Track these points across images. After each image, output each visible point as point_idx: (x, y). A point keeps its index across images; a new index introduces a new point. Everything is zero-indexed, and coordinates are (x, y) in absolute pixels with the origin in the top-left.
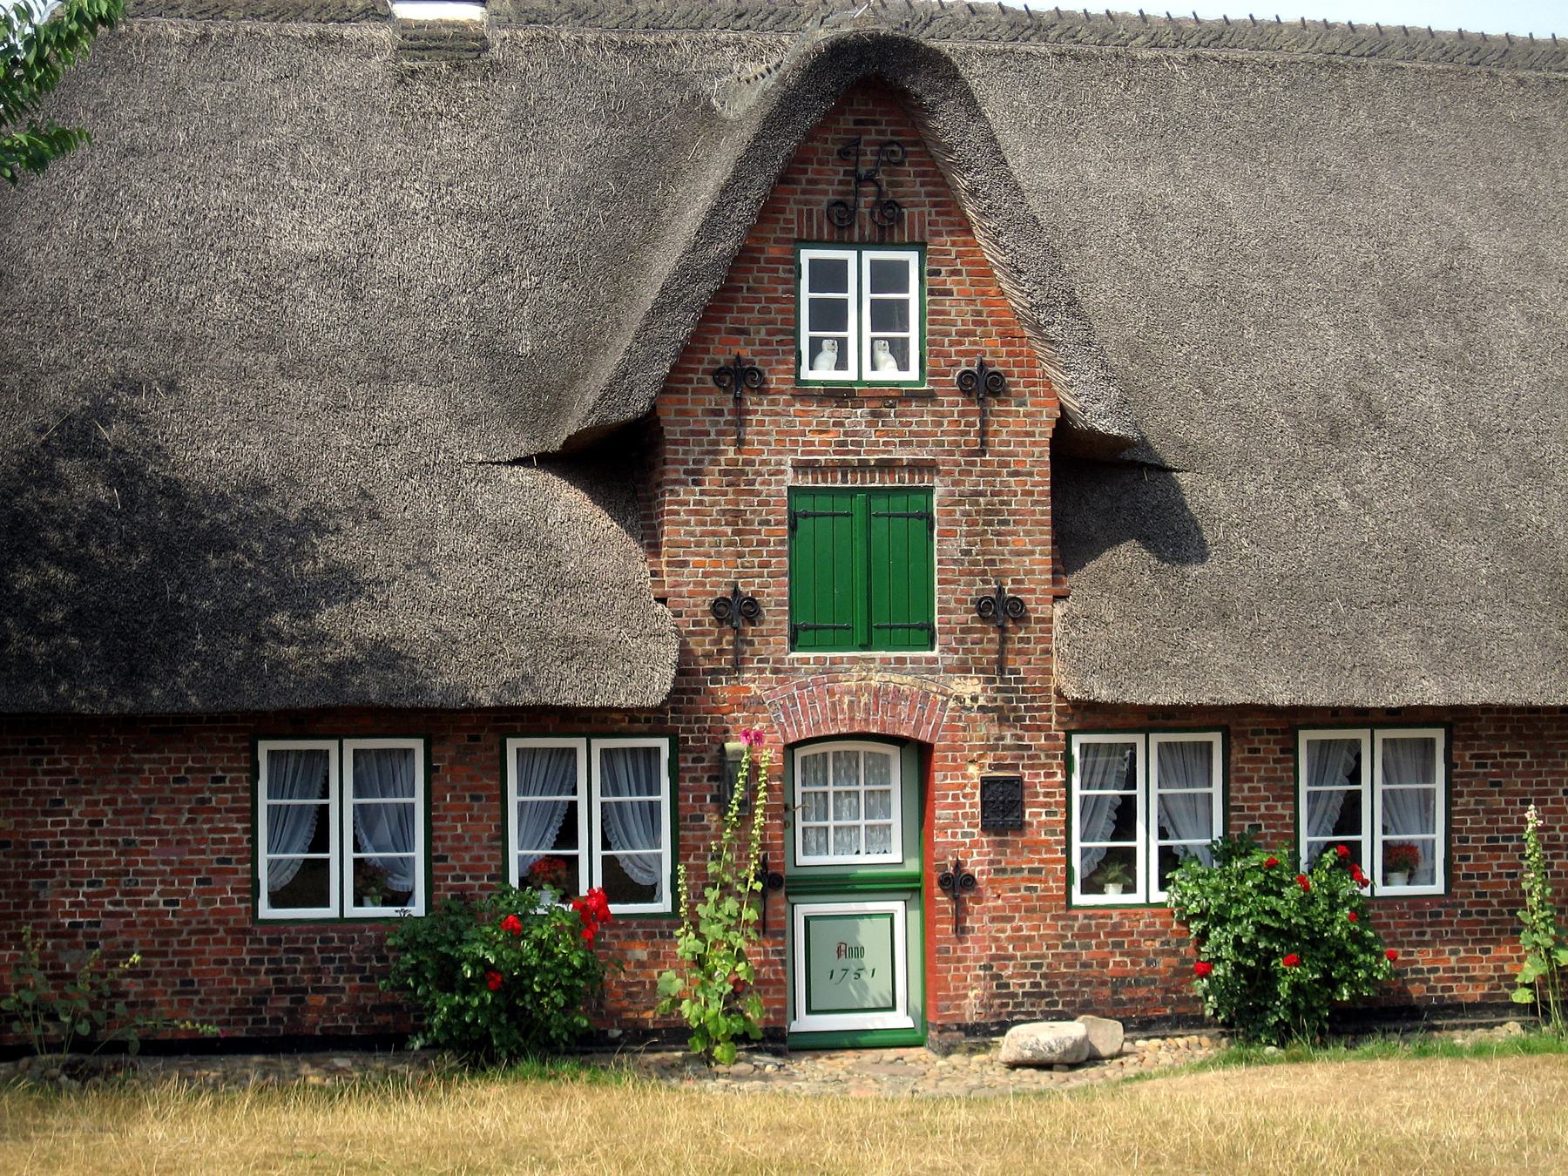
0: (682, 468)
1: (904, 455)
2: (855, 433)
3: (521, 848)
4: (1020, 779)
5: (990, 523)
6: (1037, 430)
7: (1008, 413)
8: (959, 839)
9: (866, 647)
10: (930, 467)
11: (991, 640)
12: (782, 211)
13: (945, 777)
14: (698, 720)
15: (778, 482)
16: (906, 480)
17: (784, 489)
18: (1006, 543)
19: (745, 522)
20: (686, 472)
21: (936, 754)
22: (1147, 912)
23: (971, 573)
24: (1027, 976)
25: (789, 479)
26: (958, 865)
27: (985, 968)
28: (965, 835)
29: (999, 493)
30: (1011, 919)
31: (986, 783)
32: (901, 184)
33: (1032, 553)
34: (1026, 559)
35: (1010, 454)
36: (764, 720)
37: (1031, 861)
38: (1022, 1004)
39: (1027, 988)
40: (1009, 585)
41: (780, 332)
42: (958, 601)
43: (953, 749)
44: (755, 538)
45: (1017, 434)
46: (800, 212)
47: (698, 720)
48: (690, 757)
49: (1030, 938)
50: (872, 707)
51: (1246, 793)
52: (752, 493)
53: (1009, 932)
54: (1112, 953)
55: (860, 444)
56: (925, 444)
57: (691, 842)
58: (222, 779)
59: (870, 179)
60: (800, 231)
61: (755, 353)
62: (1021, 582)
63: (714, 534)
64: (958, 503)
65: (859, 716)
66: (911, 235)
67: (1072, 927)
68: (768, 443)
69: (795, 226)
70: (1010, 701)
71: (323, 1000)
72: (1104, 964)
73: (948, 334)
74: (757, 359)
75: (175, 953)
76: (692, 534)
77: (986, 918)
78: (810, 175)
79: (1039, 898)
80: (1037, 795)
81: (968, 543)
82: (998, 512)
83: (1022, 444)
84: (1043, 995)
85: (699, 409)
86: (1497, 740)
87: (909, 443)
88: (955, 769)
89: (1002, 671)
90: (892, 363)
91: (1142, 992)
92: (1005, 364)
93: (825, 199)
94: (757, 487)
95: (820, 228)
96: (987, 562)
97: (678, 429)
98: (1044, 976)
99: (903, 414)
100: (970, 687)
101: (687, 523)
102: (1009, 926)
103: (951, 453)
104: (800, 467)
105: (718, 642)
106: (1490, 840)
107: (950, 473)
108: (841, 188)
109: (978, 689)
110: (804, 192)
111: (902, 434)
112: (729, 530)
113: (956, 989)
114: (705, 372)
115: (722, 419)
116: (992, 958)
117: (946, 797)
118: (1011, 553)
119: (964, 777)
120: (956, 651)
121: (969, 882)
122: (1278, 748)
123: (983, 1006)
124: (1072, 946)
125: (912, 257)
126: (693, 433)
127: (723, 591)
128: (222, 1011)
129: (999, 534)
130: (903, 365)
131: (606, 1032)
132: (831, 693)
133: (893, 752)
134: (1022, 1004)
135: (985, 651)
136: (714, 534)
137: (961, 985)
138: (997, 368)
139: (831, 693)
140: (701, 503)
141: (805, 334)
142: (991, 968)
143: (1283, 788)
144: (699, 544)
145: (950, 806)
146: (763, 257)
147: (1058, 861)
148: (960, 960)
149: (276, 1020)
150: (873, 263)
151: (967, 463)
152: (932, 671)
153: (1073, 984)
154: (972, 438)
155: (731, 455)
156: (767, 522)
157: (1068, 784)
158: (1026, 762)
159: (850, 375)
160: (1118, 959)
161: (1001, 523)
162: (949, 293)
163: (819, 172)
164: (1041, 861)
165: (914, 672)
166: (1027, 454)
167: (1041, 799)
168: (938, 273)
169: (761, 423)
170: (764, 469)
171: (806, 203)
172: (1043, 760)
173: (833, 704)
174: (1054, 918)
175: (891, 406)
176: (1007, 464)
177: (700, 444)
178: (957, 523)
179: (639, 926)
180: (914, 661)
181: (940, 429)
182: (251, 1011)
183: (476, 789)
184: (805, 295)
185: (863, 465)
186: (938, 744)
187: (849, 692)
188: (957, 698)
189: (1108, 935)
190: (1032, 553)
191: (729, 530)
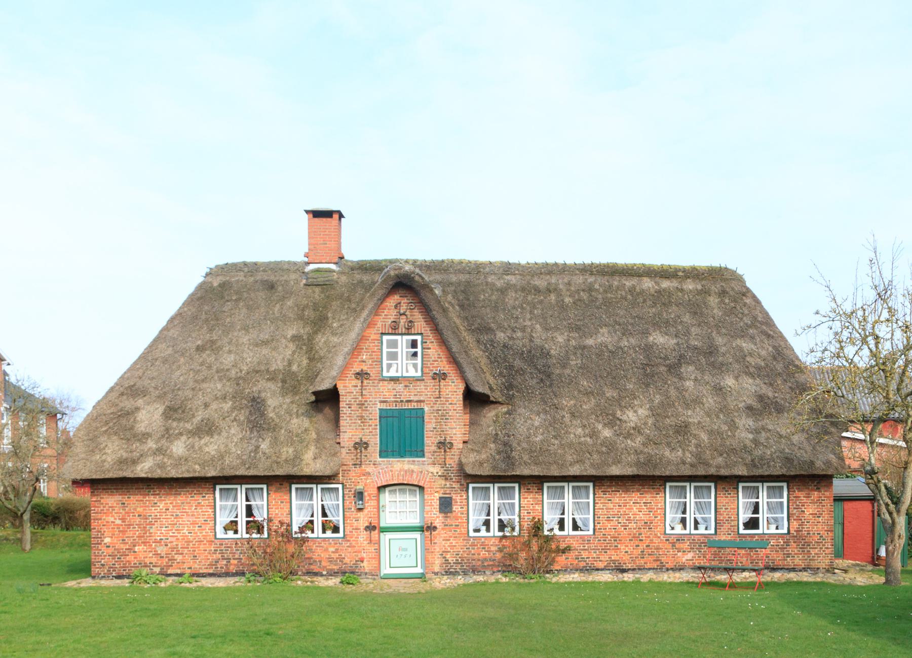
1: (416, 399)
4: (451, 498)
9: (402, 457)
10: (423, 401)
16: (414, 405)
25: (379, 406)
31: (440, 498)
59: (404, 314)
71: (236, 562)
90: (413, 370)
91: (491, 563)
104: (381, 402)
121: (435, 528)
125: (419, 338)
127: (358, 440)
130: (416, 371)
133: (417, 489)
141: (385, 362)
157: (468, 499)
159: (399, 374)
181: (426, 391)
184: (385, 350)
185: (402, 401)
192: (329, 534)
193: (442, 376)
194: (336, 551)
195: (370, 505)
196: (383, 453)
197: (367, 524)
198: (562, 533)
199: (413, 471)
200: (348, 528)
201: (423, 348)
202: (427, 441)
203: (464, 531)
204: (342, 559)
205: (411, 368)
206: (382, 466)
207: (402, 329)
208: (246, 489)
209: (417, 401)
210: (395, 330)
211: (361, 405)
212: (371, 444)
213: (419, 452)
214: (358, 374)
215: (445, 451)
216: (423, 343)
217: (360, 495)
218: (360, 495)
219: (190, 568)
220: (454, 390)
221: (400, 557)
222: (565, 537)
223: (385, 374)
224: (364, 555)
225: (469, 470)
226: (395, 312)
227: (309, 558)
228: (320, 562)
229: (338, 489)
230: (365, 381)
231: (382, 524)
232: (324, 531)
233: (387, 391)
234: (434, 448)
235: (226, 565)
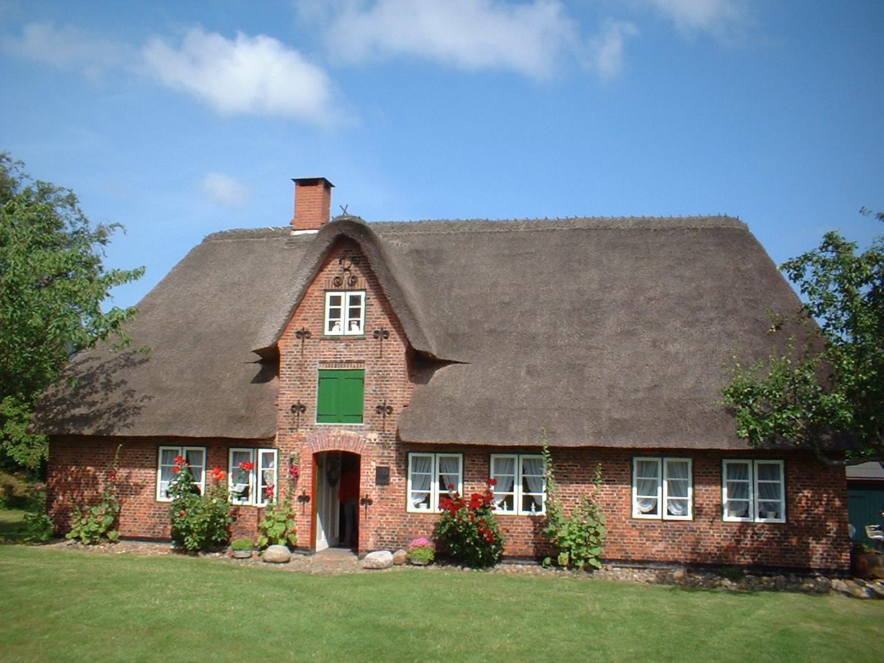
1: (355, 359)
5: (382, 381)
8: (369, 487)
10: (363, 362)
11: (381, 420)
15: (315, 368)
17: (316, 370)
19: (304, 381)
20: (287, 365)
21: (362, 458)
22: (433, 516)
26: (367, 496)
27: (376, 531)
28: (370, 486)
29: (386, 371)
31: (378, 468)
35: (391, 358)
39: (390, 539)
40: (388, 402)
41: (318, 319)
42: (371, 407)
43: (367, 456)
44: (306, 385)
45: (393, 351)
47: (286, 444)
49: (391, 522)
51: (470, 476)
53: (384, 520)
57: (283, 484)
58: (147, 458)
61: (310, 326)
62: (392, 401)
65: (337, 444)
66: (361, 286)
70: (386, 441)
73: (371, 318)
75: (133, 510)
76: (286, 384)
77: (377, 514)
79: (395, 508)
82: (386, 377)
83: (395, 354)
86: (566, 460)
89: (384, 431)
93: (334, 277)
94: (308, 369)
98: (396, 535)
100: (374, 436)
101: (285, 381)
102: (384, 517)
104: (321, 362)
106: (563, 497)
109: (376, 437)
111: (355, 352)
114: (294, 333)
116: (378, 528)
117: (364, 472)
118: (390, 391)
119: (371, 466)
120: (369, 424)
122: (482, 460)
123: (374, 544)
124: (406, 526)
125: (363, 294)
126: (289, 352)
128: (143, 529)
132: (328, 437)
135: (379, 424)
136: (294, 384)
139: (328, 437)
141: (327, 320)
143: (484, 475)
144: (289, 387)
146: (313, 296)
147: (402, 496)
149: (159, 532)
152: (361, 430)
153: (405, 539)
154: (378, 352)
155: (300, 359)
156: (310, 381)
159: (341, 333)
160: (422, 531)
162: (372, 305)
164: (396, 496)
165: (354, 431)
168: (369, 298)
171: (328, 278)
176: (389, 361)
177: (291, 356)
180: (356, 427)
182: (152, 529)
185: (342, 362)
186: (362, 454)
187: (334, 436)
188: (369, 440)
189: (419, 523)
191: (298, 383)
193: (386, 334)
196: (320, 417)
198: (510, 513)
201: (366, 305)
202: (367, 405)
203: (401, 505)
207: (345, 285)
208: (187, 451)
209: (357, 362)
210: (338, 284)
213: (359, 417)
214: (298, 333)
215: (384, 416)
216: (366, 299)
219: (129, 531)
220: (396, 351)
222: (512, 518)
223: (327, 332)
224: (297, 527)
225: (404, 438)
227: (241, 528)
233: (328, 352)
234: (373, 412)
235: (163, 530)
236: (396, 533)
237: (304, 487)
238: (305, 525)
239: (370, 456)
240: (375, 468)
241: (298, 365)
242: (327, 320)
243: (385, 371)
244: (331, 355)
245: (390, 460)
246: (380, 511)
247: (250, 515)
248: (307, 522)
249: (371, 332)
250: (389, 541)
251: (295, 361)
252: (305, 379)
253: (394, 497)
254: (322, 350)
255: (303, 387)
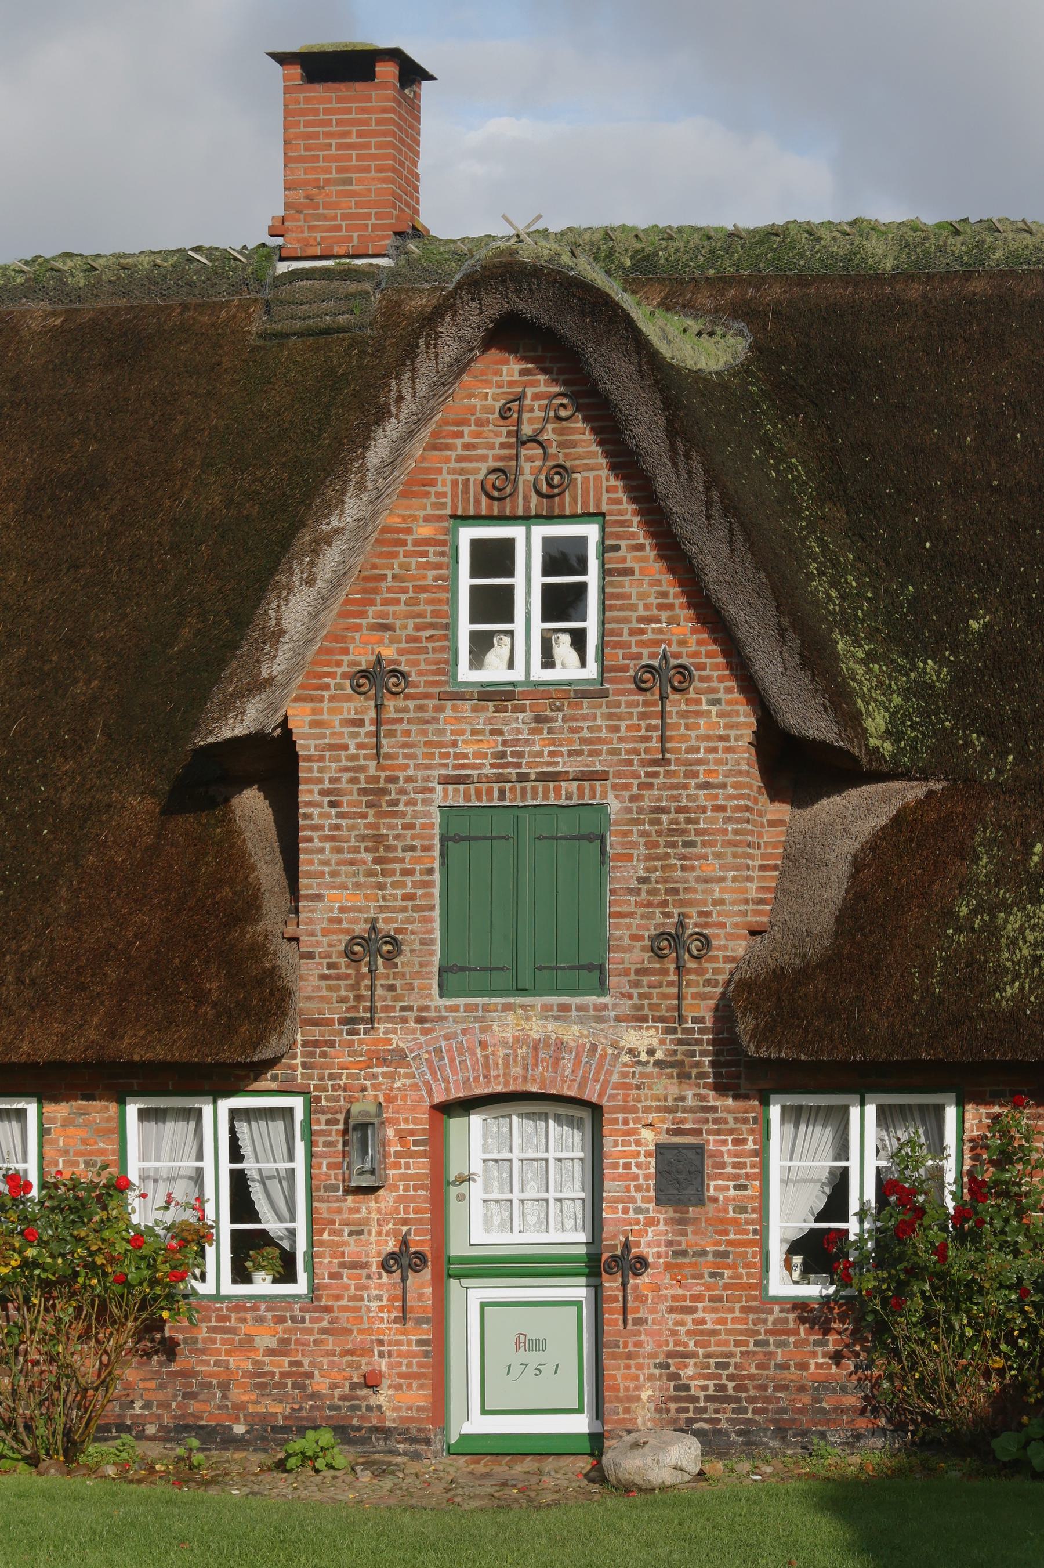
0: (316, 788)
1: (573, 766)
2: (516, 742)
3: (233, 1221)
5: (673, 845)
6: (732, 733)
7: (698, 714)
10: (603, 776)
11: (670, 984)
12: (433, 483)
13: (616, 1145)
14: (331, 1077)
18: (693, 868)
19: (388, 848)
20: (322, 793)
23: (649, 904)
24: (709, 1377)
25: (439, 796)
26: (627, 1245)
28: (638, 1210)
30: (692, 1310)
32: (574, 444)
33: (723, 879)
34: (716, 887)
35: (700, 762)
36: (407, 1076)
37: (719, 1243)
38: (704, 1410)
39: (711, 1392)
42: (635, 938)
43: (625, 1109)
45: (708, 738)
46: (455, 483)
47: (331, 1077)
48: (323, 1118)
49: (714, 1333)
50: (530, 1061)
52: (395, 814)
53: (690, 1326)
54: (814, 1354)
55: (520, 755)
56: (598, 753)
57: (325, 1215)
60: (454, 506)
61: (401, 652)
62: (707, 914)
63: (352, 863)
64: (638, 822)
66: (586, 503)
67: (765, 1322)
68: (412, 756)
69: (448, 500)
70: (692, 1054)
72: (803, 1366)
74: (403, 659)
76: (326, 863)
78: (467, 439)
79: (726, 1287)
80: (723, 1165)
81: (647, 869)
82: (684, 832)
83: (715, 750)
84: (727, 1400)
85: (337, 719)
87: (579, 753)
88: (629, 1133)
90: (573, 656)
92: (696, 654)
94: (401, 807)
95: (478, 502)
96: (668, 891)
97: (312, 743)
98: (731, 1378)
99: (574, 719)
100: (644, 1039)
101: (322, 851)
102: (689, 1318)
103: (630, 763)
104: (446, 780)
105: (355, 987)
107: (627, 787)
108: (503, 452)
109: (655, 1042)
110: (460, 459)
112: (369, 857)
113: (627, 1389)
114: (344, 675)
115: (362, 731)
116: (670, 1355)
117: (615, 1166)
118: (698, 880)
119: (638, 1143)
120: (630, 997)
121: (642, 1262)
125: (591, 531)
129: (684, 857)
130: (583, 664)
131: (230, 1428)
133: (586, 1115)
134: (704, 1410)
135: (665, 996)
136: (352, 863)
137: (632, 1384)
138: (685, 661)
139: (483, 1045)
140: (337, 827)
141: (465, 627)
142: (668, 1366)
144: (334, 874)
145: (621, 1177)
146: (410, 538)
147: (751, 1243)
148: (629, 1356)
150: (547, 541)
151: (648, 775)
152: (600, 1020)
155: (372, 771)
156: (413, 848)
157: (762, 1153)
158: (711, 1126)
159: (517, 675)
161: (687, 844)
163: (478, 435)
164: (729, 1243)
165: (581, 1021)
166: (718, 762)
167: (729, 1170)
169: (407, 733)
170: (410, 787)
171: (462, 472)
172: (731, 1124)
173: (486, 1057)
174: (743, 1309)
175: (559, 710)
176: (695, 775)
177: (337, 759)
178: (633, 845)
179: (268, 1310)
180: (580, 1008)
181: (617, 733)
183: (91, 1153)
185: (523, 778)
187: (504, 1043)
188: (630, 1051)
190: (723, 879)
191: (369, 857)
192: (263, 1285)
194: (282, 1349)
195: (405, 1174)
196: (454, 977)
197: (391, 1246)
199: (560, 1045)
200: (326, 1262)
202: (619, 932)
204: (301, 1378)
205: (563, 648)
206: (451, 1027)
210: (498, 500)
211: (375, 794)
212: (411, 942)
213: (593, 975)
214: (364, 674)
216: (604, 549)
217: (359, 1133)
218: (359, 1133)
220: (718, 727)
221: (512, 1376)
223: (465, 673)
224: (383, 1365)
226: (499, 434)
228: (224, 1386)
229: (291, 1110)
230: (390, 704)
231: (457, 1248)
232: (241, 1275)
233: (471, 739)
234: (638, 956)
236: (731, 1370)
237: (405, 1222)
238: (414, 1355)
239: (634, 1110)
240: (652, 1148)
241: (363, 792)
242: (465, 627)
243: (679, 810)
244: (484, 755)
245: (707, 1121)
246: (674, 1298)
247: (212, 1330)
248: (420, 1343)
249: (625, 669)
250: (708, 1398)
251: (354, 780)
252: (391, 842)
253: (723, 1248)
254: (449, 737)
255: (385, 873)
